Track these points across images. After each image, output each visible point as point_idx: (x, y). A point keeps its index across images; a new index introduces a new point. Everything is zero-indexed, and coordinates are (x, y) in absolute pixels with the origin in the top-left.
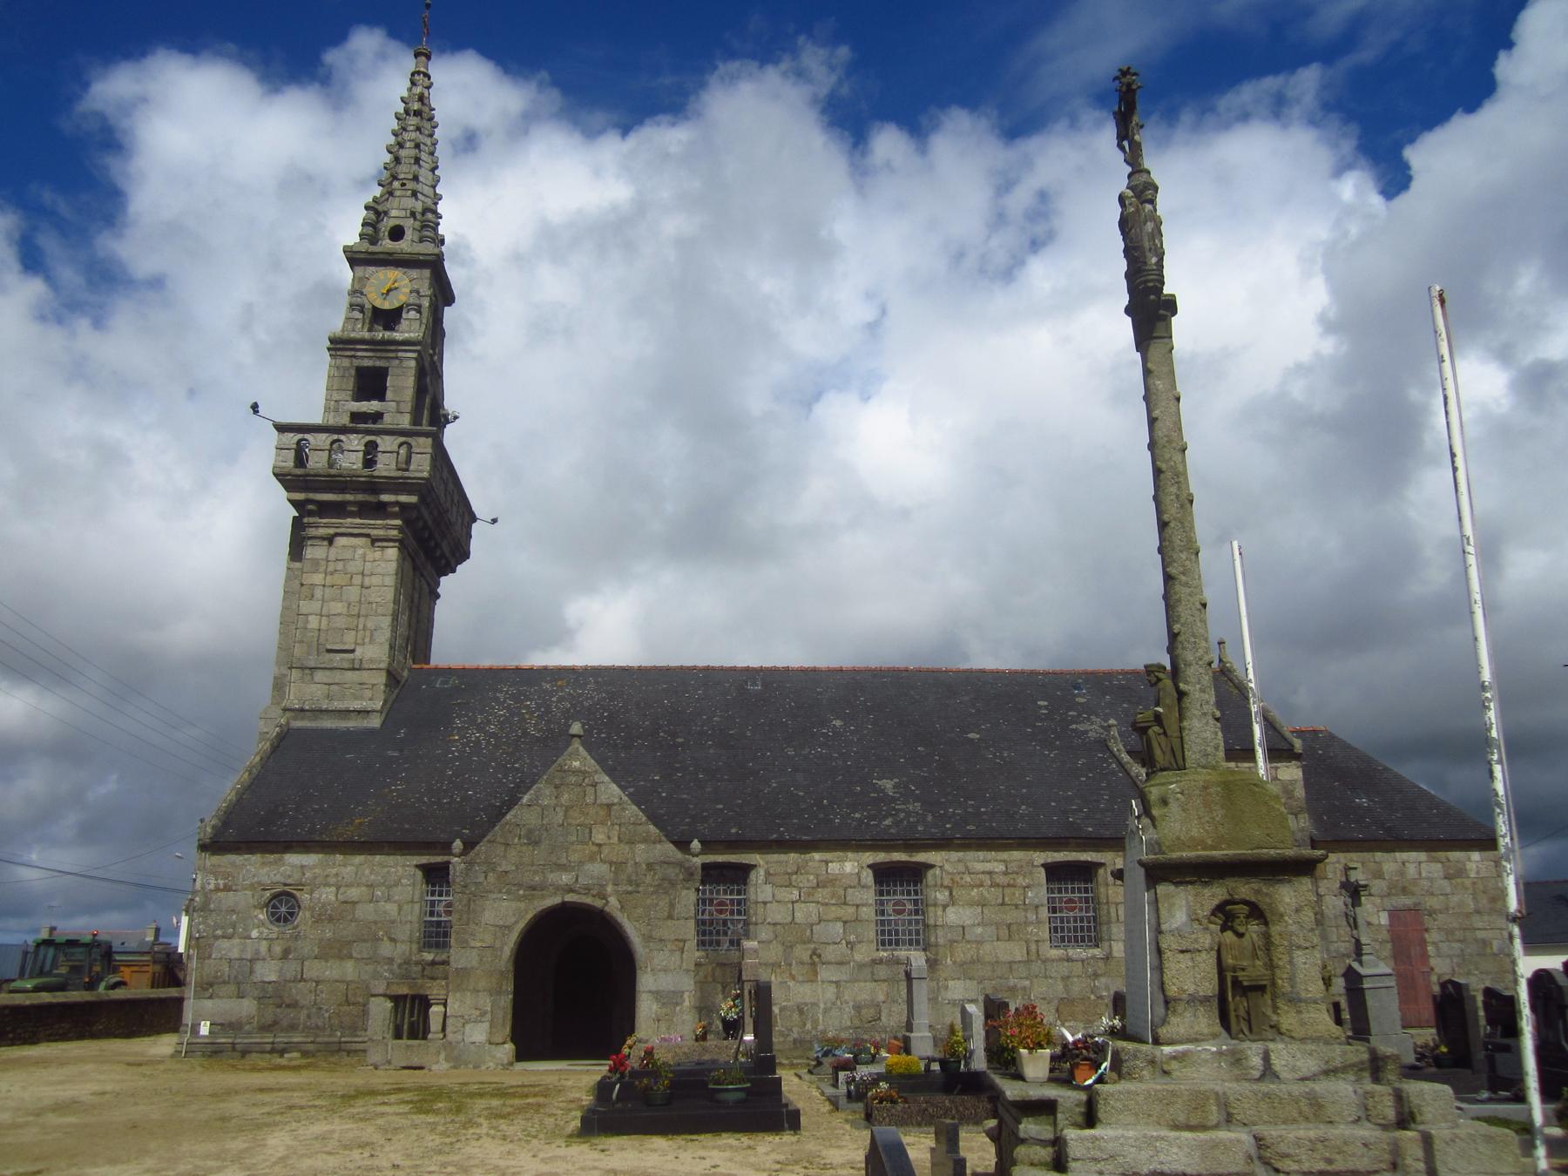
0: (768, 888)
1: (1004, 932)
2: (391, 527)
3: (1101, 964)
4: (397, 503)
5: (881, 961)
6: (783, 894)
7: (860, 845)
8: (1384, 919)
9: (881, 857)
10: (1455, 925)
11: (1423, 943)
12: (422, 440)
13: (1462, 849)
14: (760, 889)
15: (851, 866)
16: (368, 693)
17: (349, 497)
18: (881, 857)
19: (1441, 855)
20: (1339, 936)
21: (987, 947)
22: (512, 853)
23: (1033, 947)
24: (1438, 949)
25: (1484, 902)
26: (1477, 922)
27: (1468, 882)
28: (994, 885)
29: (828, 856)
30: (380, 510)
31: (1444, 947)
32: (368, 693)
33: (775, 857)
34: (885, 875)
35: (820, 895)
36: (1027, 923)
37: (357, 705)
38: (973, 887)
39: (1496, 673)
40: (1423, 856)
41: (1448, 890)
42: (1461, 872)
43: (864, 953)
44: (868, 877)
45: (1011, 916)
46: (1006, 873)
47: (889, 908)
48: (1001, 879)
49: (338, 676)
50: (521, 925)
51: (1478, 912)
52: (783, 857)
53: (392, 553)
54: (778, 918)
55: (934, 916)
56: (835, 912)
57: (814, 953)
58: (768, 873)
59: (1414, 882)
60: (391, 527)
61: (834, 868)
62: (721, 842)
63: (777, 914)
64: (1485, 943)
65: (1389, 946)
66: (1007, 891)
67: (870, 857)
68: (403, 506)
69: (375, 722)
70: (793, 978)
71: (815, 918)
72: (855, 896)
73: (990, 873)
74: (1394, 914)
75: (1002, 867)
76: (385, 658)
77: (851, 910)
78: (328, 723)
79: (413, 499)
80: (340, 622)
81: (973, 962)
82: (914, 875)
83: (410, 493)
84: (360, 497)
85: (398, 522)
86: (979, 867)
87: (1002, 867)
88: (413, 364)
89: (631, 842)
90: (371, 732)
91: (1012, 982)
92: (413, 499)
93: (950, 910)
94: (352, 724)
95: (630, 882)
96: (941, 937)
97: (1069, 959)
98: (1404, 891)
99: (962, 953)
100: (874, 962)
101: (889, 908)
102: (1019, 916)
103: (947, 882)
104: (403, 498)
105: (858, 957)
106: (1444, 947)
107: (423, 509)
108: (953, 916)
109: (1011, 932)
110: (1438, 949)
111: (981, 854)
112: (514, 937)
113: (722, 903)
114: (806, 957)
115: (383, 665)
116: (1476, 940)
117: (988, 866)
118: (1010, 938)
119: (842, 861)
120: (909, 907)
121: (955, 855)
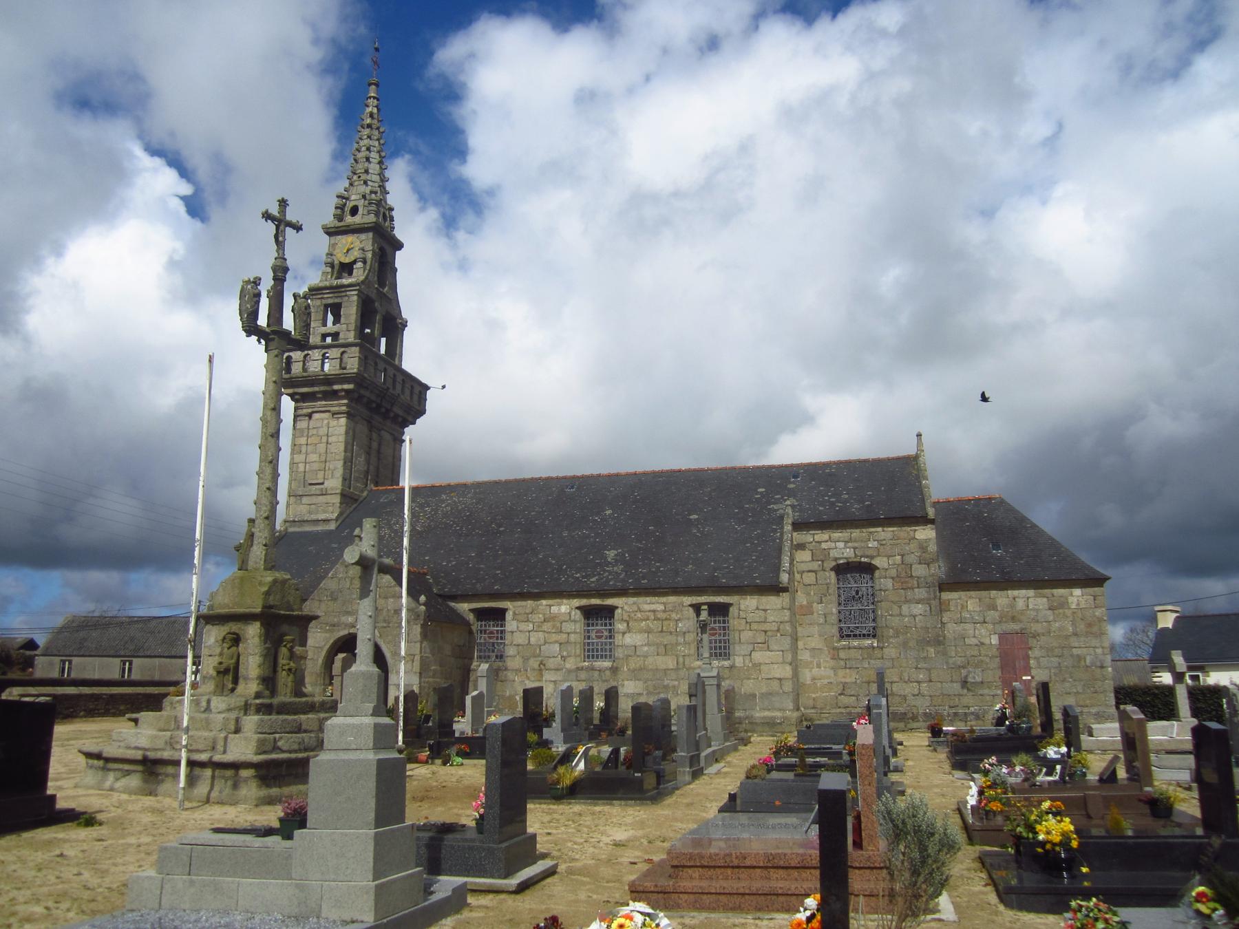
0: (514, 623)
1: (662, 650)
2: (341, 405)
3: (726, 671)
4: (343, 390)
5: (582, 669)
6: (523, 626)
7: (570, 595)
8: (995, 640)
9: (584, 602)
10: (1055, 644)
11: (1027, 657)
12: (353, 349)
13: (1064, 587)
14: (511, 624)
15: (564, 607)
16: (331, 509)
17: (316, 389)
18: (584, 602)
19: (1047, 591)
20: (956, 652)
21: (650, 659)
22: (323, 606)
23: (681, 660)
24: (1039, 663)
25: (1082, 627)
26: (1074, 642)
27: (1069, 613)
28: (657, 619)
29: (550, 602)
30: (334, 395)
31: (1044, 661)
32: (331, 509)
33: (519, 603)
34: (590, 613)
35: (546, 627)
36: (677, 644)
37: (322, 516)
38: (642, 620)
39: (206, 533)
40: (1031, 593)
41: (1051, 618)
42: (1064, 604)
43: (570, 664)
44: (577, 615)
45: (667, 639)
46: (664, 611)
47: (593, 635)
48: (664, 616)
49: (314, 500)
50: (327, 647)
51: (1075, 634)
52: (524, 603)
53: (343, 421)
54: (520, 641)
55: (618, 639)
56: (554, 637)
57: (541, 663)
58: (514, 614)
59: (1022, 612)
60: (341, 405)
61: (554, 609)
62: (486, 595)
63: (520, 639)
64: (1080, 658)
65: (998, 660)
66: (665, 623)
67: (577, 602)
68: (347, 391)
69: (333, 526)
70: (528, 678)
71: (542, 642)
72: (569, 627)
73: (654, 611)
74: (1003, 637)
75: (662, 607)
76: (340, 487)
77: (565, 636)
78: (308, 528)
79: (351, 386)
80: (316, 466)
81: (641, 669)
82: (720, 611)
83: (349, 383)
84: (322, 388)
85: (345, 401)
86: (647, 607)
87: (662, 607)
88: (355, 298)
89: (386, 598)
90: (331, 531)
91: (666, 682)
92: (351, 386)
93: (627, 635)
94: (320, 528)
95: (385, 621)
96: (619, 653)
97: (593, 669)
98: (1013, 619)
99: (634, 663)
100: (578, 669)
101: (593, 635)
102: (672, 639)
103: (626, 617)
104: (346, 387)
105: (568, 666)
106: (1044, 661)
107: (362, 392)
108: (629, 639)
109: (667, 650)
110: (1039, 663)
111: (648, 599)
112: (324, 653)
113: (492, 633)
114: (536, 666)
115: (338, 491)
116: (1072, 656)
117: (653, 607)
118: (666, 654)
119: (560, 605)
120: (606, 633)
121: (631, 600)
